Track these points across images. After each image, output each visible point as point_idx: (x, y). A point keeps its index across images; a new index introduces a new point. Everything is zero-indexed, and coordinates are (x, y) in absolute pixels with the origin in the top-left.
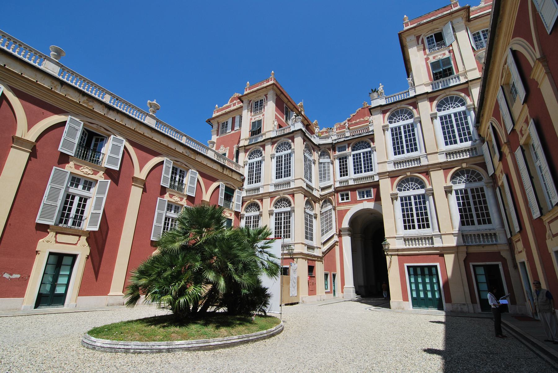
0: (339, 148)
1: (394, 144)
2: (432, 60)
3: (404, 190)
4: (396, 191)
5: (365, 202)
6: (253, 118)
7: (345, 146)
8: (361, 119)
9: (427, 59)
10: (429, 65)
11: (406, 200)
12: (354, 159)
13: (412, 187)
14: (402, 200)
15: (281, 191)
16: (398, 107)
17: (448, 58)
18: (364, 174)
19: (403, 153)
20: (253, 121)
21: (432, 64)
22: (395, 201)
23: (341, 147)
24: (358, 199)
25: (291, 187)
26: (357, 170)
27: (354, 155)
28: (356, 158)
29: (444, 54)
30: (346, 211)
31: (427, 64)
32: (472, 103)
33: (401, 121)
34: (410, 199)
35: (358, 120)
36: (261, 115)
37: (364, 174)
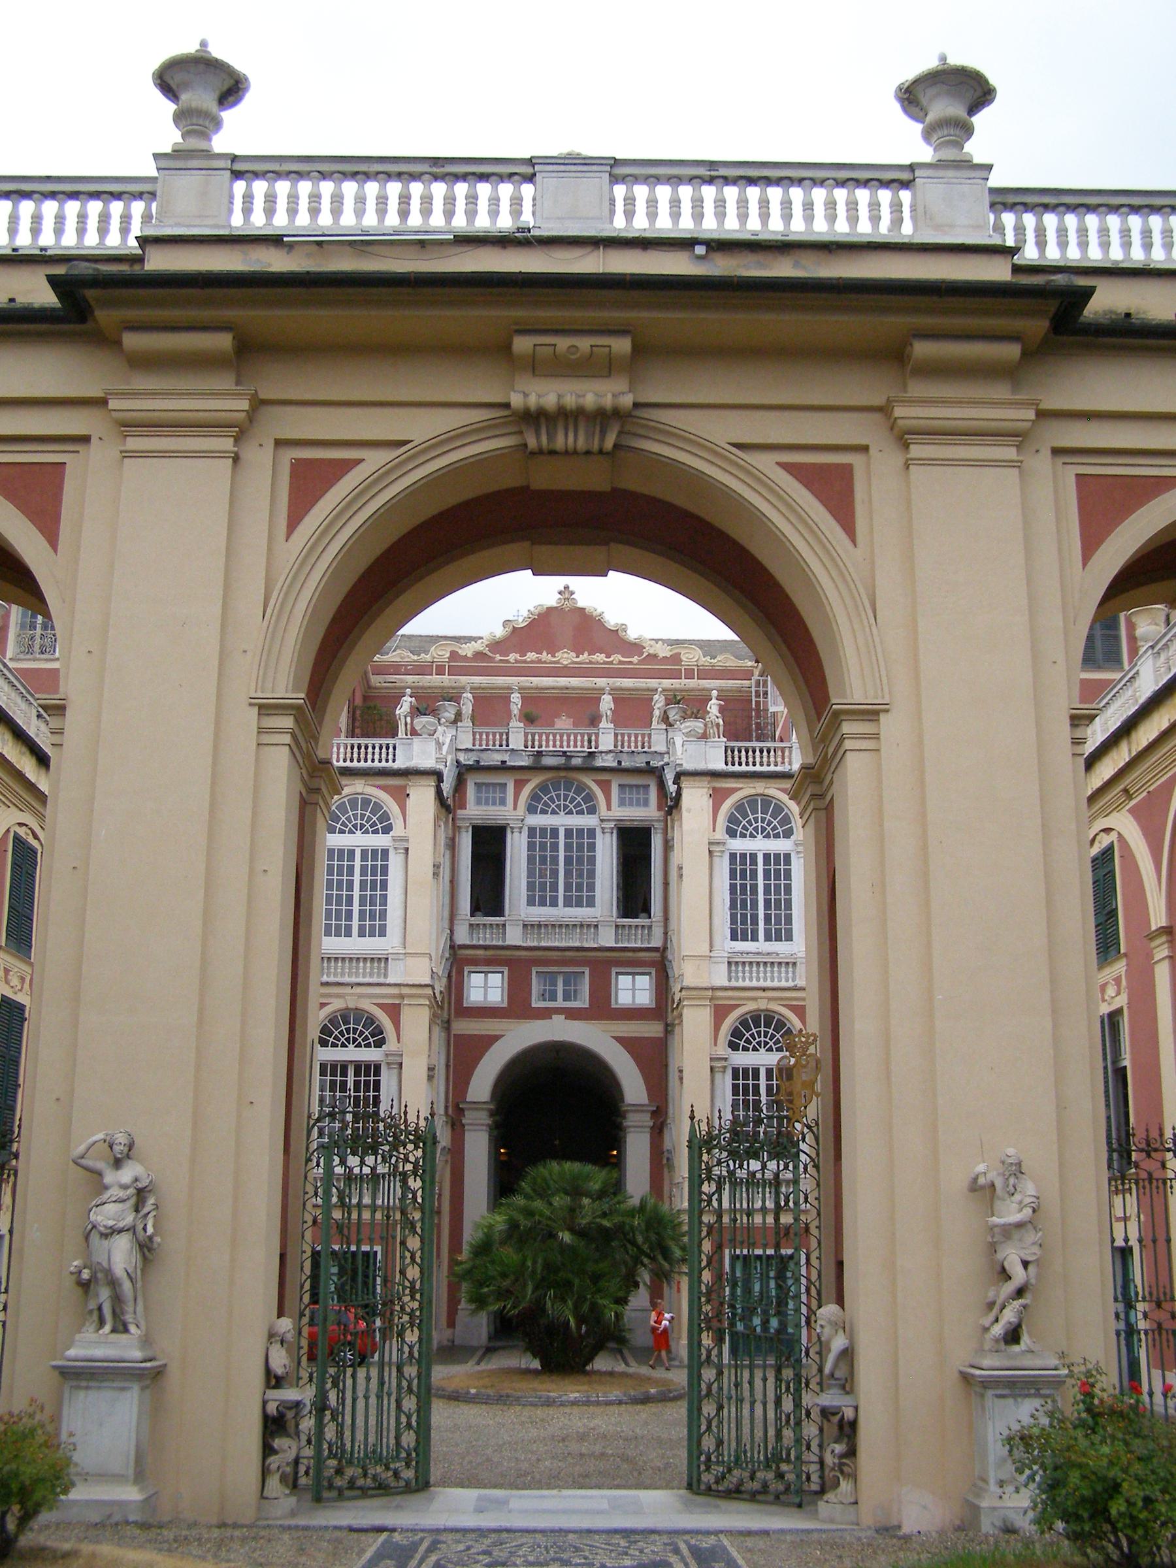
1: (733, 905)
3: (745, 1049)
4: (723, 1050)
5: (558, 1019)
8: (545, 656)
11: (746, 1078)
12: (531, 847)
13: (766, 1043)
14: (735, 1076)
15: (352, 985)
16: (760, 791)
18: (562, 913)
19: (755, 938)
22: (718, 1076)
23: (487, 785)
24: (535, 1004)
25: (390, 980)
26: (540, 894)
27: (532, 831)
28: (542, 840)
30: (490, 1040)
33: (760, 836)
34: (756, 1076)
35: (531, 656)
37: (562, 913)
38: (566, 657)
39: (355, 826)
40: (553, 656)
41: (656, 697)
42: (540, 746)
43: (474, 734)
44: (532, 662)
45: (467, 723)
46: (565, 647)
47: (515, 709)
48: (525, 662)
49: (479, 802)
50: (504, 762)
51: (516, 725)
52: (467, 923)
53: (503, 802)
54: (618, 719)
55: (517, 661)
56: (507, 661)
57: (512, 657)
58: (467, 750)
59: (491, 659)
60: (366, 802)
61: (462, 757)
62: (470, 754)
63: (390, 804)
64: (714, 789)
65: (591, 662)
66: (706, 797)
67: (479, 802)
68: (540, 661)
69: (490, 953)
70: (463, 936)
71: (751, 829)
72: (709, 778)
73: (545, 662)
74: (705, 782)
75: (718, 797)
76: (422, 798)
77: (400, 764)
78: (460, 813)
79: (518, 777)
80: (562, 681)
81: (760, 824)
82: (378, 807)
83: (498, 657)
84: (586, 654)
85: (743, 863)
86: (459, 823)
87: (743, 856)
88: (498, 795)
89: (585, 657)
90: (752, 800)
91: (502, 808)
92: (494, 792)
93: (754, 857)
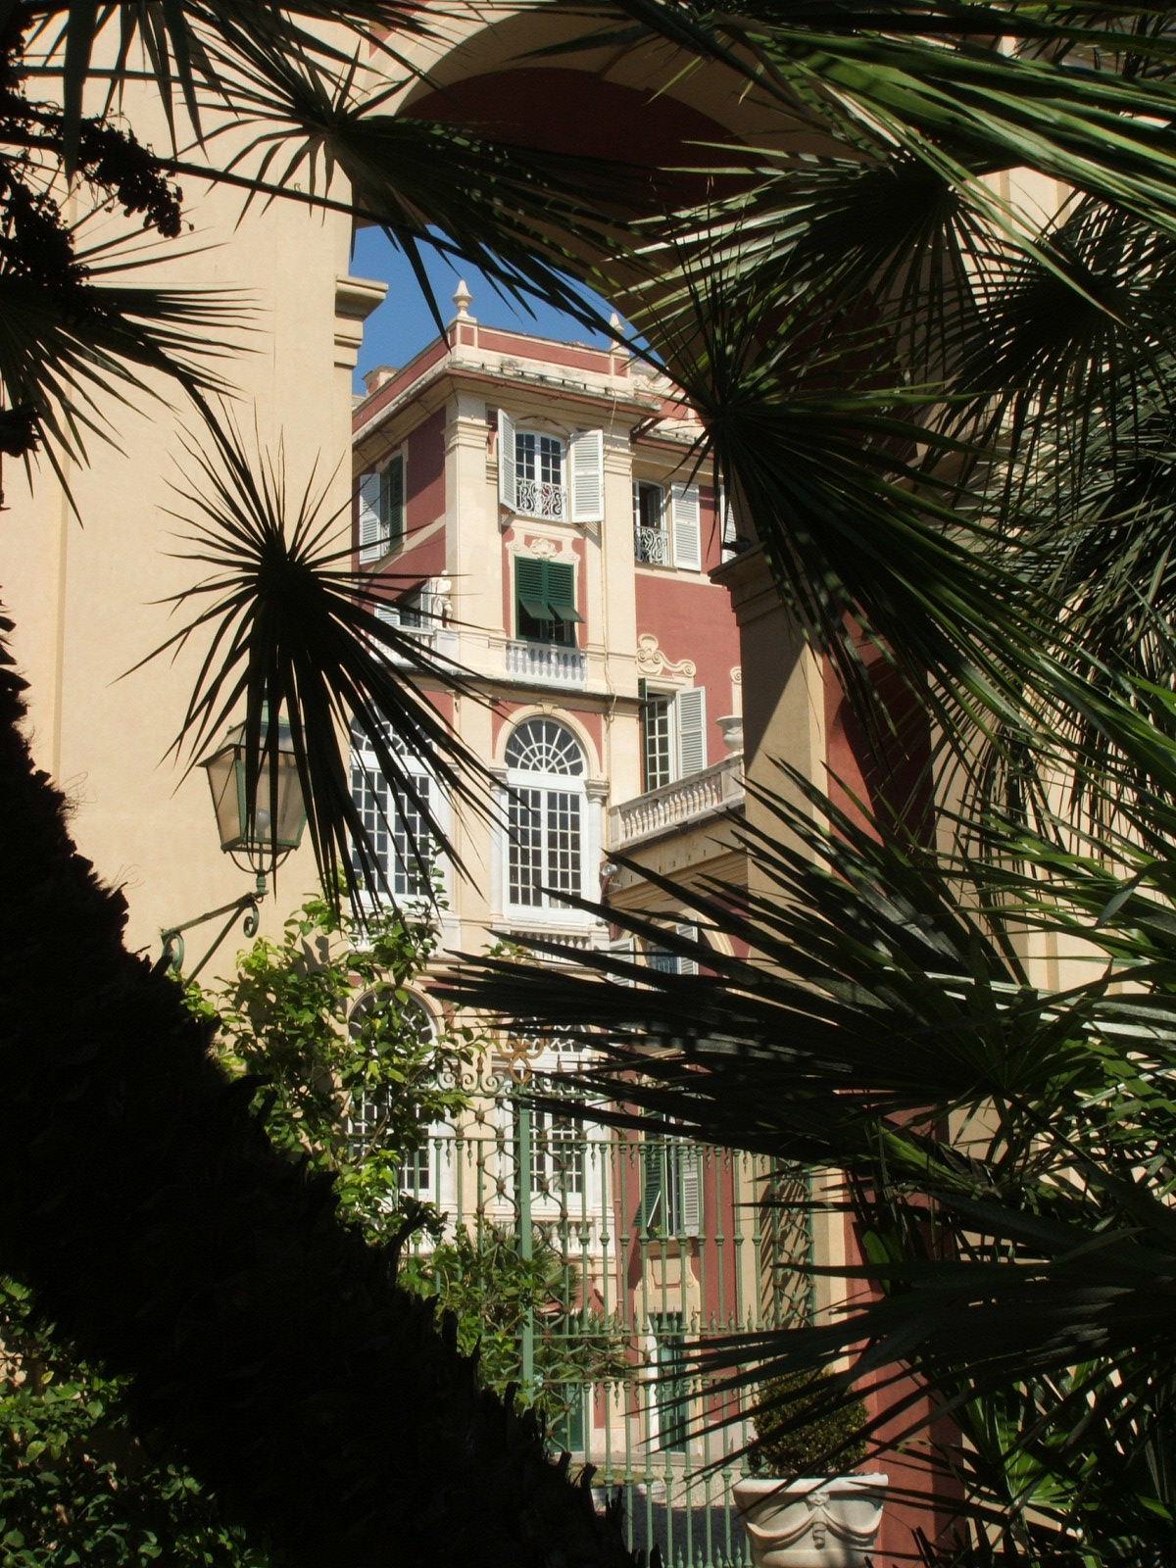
17: (568, 569)
21: (522, 564)
29: (559, 546)
31: (505, 552)
32: (603, 778)
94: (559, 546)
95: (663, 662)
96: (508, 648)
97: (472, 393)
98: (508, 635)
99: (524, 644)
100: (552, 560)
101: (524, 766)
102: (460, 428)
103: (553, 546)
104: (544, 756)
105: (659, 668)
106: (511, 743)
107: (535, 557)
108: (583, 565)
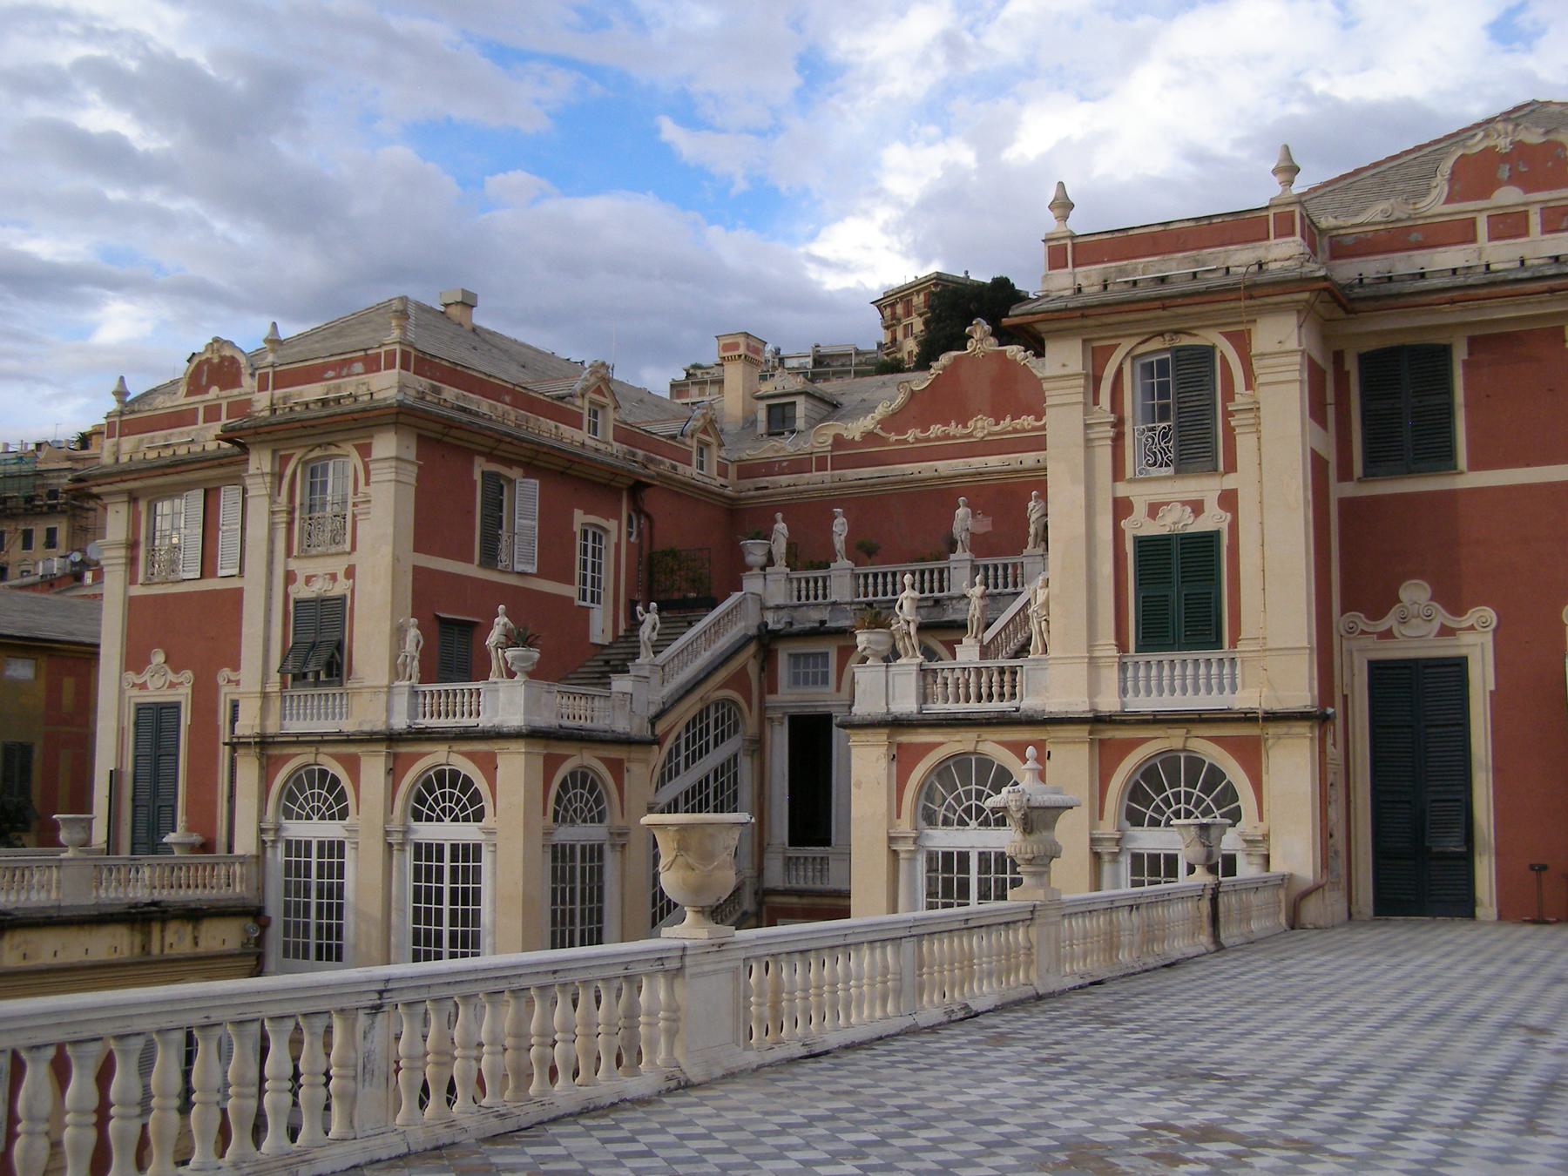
0: (795, 657)
2: (1140, 525)
6: (301, 567)
7: (826, 655)
8: (954, 429)
9: (1122, 508)
10: (1129, 548)
20: (301, 591)
21: (1141, 542)
23: (807, 656)
29: (1197, 507)
32: (1262, 829)
33: (973, 823)
35: (936, 430)
36: (339, 565)
38: (981, 426)
39: (443, 810)
40: (965, 426)
41: (1031, 504)
42: (875, 594)
43: (791, 580)
44: (937, 438)
45: (781, 567)
46: (979, 412)
47: (839, 542)
48: (928, 439)
49: (795, 681)
50: (823, 622)
51: (842, 565)
52: (780, 857)
53: (825, 681)
54: (981, 546)
55: (917, 440)
56: (905, 441)
57: (911, 434)
58: (778, 608)
59: (884, 441)
60: (455, 774)
61: (770, 618)
62: (781, 613)
63: (480, 783)
64: (900, 746)
65: (1015, 431)
66: (884, 763)
67: (795, 681)
68: (947, 437)
69: (805, 901)
70: (775, 876)
71: (960, 810)
72: (886, 731)
73: (954, 437)
74: (882, 736)
75: (903, 759)
76: (514, 765)
77: (485, 721)
78: (771, 699)
79: (842, 643)
80: (977, 463)
81: (973, 802)
82: (468, 782)
83: (893, 437)
84: (1008, 419)
85: (947, 867)
86: (770, 714)
87: (948, 856)
88: (820, 669)
89: (1006, 423)
90: (961, 760)
91: (820, 689)
92: (815, 666)
93: (964, 857)
94: (1197, 507)
95: (1442, 617)
96: (1123, 667)
97: (1061, 334)
98: (1122, 646)
99: (1143, 658)
100: (1190, 530)
101: (1155, 823)
102: (1045, 386)
103: (1189, 509)
104: (1182, 806)
105: (1436, 625)
106: (1135, 793)
107: (1165, 531)
108: (1234, 527)
